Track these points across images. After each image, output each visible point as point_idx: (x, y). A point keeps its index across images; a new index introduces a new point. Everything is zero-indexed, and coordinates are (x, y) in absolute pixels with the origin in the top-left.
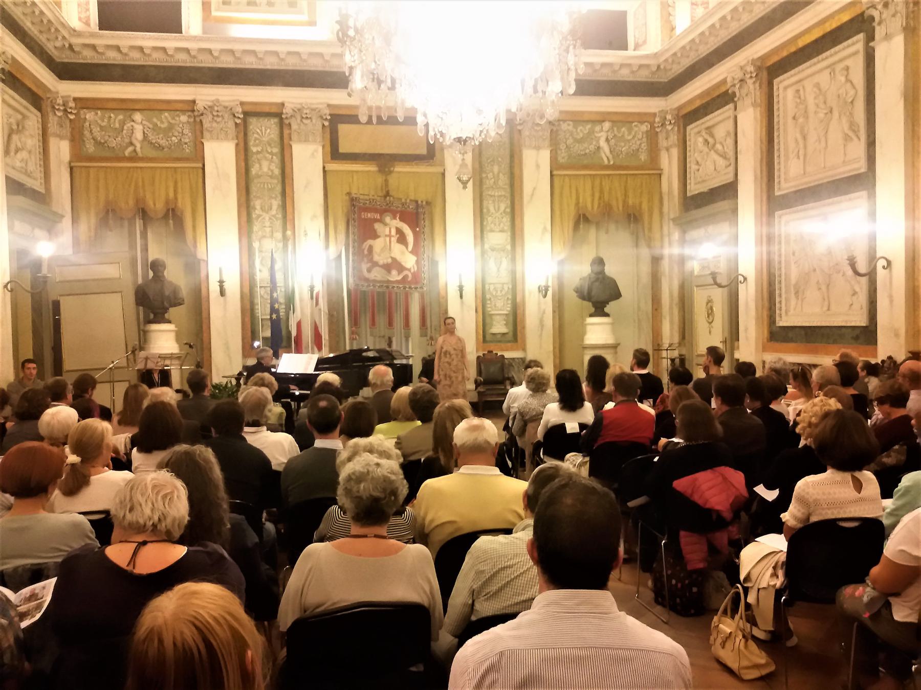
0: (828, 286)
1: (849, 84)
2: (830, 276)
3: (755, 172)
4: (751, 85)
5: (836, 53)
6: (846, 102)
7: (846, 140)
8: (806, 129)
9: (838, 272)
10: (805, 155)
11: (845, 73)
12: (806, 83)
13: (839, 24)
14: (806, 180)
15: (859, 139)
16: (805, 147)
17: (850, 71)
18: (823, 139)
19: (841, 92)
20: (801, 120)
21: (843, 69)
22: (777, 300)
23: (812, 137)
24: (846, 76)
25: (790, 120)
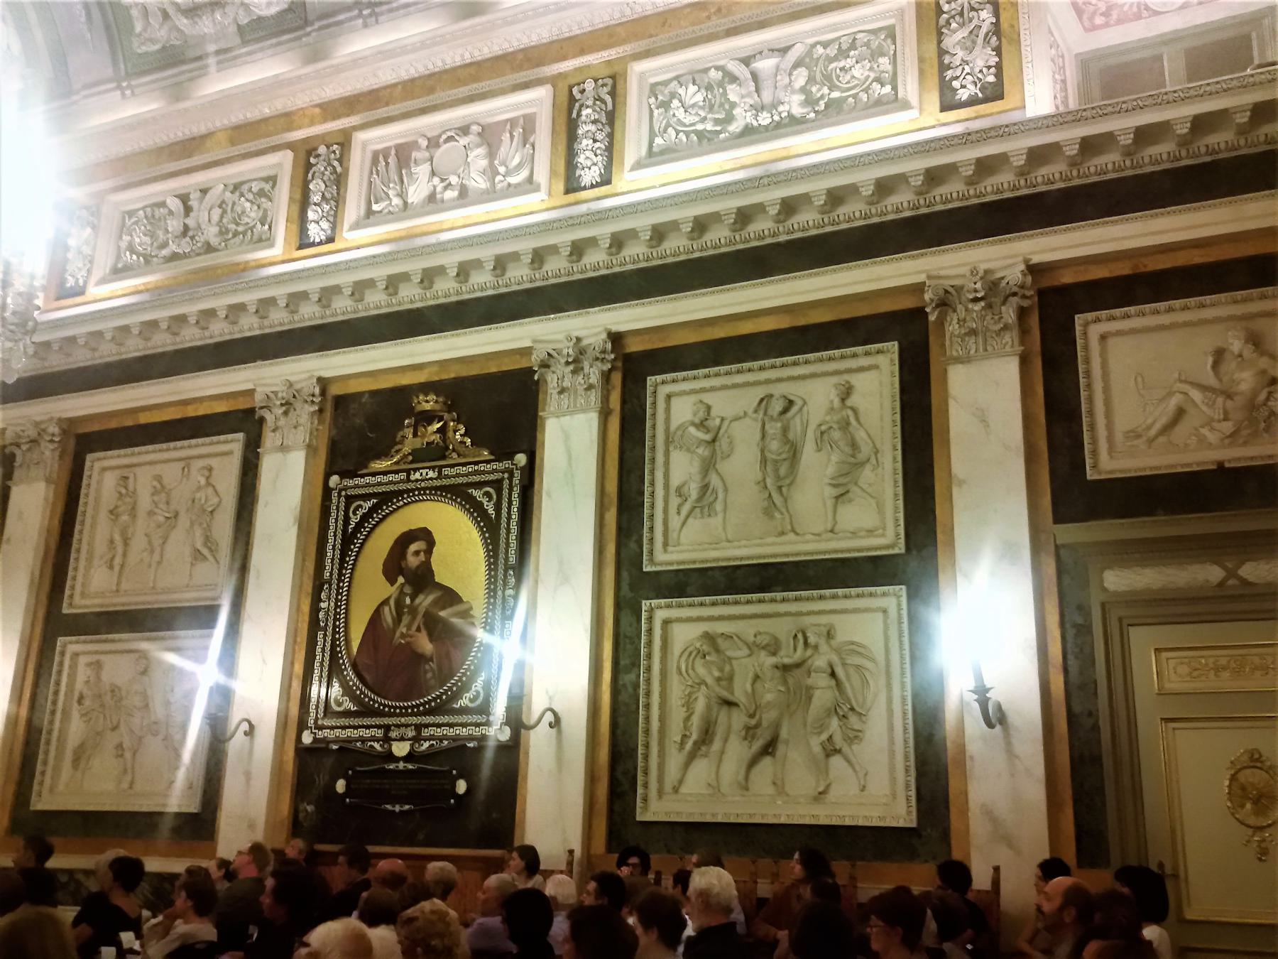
0: (134, 754)
1: (210, 490)
2: (140, 738)
3: (32, 573)
4: (48, 452)
5: (197, 446)
6: (204, 511)
7: (196, 559)
8: (130, 531)
9: (155, 734)
10: (122, 566)
11: (207, 473)
12: (138, 470)
13: (209, 412)
14: (116, 600)
15: (217, 562)
16: (125, 555)
17: (214, 473)
18: (158, 551)
19: (198, 495)
20: (125, 518)
21: (203, 468)
22: (39, 767)
23: (139, 543)
24: (208, 478)
25: (103, 515)
